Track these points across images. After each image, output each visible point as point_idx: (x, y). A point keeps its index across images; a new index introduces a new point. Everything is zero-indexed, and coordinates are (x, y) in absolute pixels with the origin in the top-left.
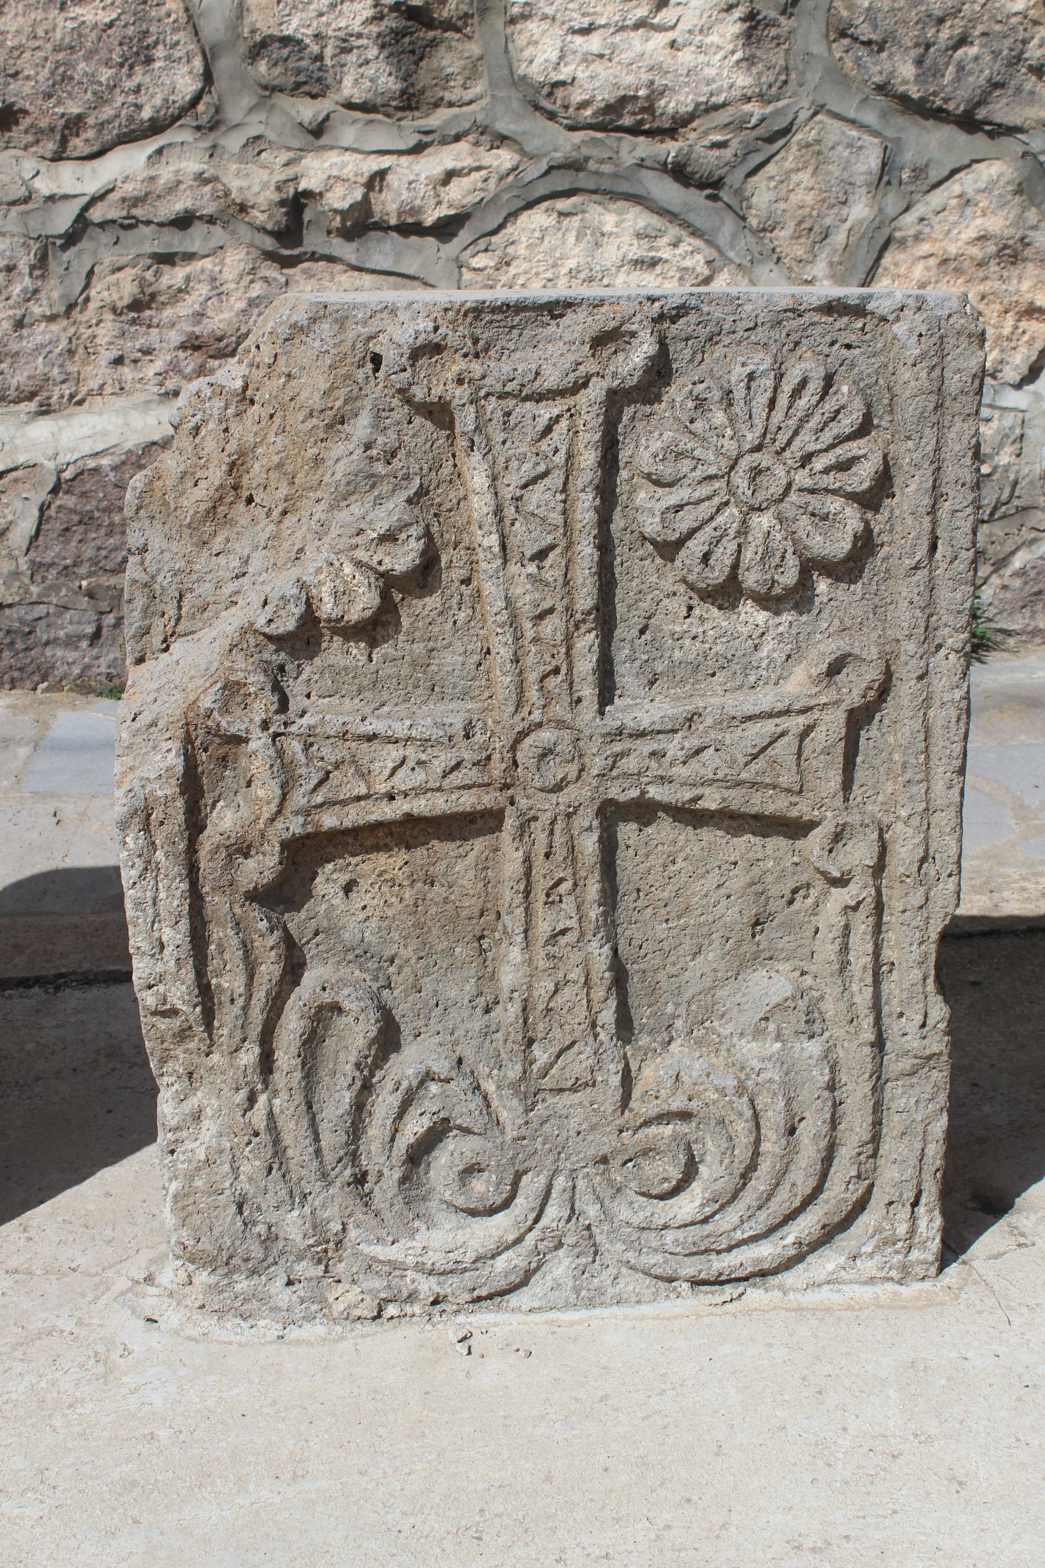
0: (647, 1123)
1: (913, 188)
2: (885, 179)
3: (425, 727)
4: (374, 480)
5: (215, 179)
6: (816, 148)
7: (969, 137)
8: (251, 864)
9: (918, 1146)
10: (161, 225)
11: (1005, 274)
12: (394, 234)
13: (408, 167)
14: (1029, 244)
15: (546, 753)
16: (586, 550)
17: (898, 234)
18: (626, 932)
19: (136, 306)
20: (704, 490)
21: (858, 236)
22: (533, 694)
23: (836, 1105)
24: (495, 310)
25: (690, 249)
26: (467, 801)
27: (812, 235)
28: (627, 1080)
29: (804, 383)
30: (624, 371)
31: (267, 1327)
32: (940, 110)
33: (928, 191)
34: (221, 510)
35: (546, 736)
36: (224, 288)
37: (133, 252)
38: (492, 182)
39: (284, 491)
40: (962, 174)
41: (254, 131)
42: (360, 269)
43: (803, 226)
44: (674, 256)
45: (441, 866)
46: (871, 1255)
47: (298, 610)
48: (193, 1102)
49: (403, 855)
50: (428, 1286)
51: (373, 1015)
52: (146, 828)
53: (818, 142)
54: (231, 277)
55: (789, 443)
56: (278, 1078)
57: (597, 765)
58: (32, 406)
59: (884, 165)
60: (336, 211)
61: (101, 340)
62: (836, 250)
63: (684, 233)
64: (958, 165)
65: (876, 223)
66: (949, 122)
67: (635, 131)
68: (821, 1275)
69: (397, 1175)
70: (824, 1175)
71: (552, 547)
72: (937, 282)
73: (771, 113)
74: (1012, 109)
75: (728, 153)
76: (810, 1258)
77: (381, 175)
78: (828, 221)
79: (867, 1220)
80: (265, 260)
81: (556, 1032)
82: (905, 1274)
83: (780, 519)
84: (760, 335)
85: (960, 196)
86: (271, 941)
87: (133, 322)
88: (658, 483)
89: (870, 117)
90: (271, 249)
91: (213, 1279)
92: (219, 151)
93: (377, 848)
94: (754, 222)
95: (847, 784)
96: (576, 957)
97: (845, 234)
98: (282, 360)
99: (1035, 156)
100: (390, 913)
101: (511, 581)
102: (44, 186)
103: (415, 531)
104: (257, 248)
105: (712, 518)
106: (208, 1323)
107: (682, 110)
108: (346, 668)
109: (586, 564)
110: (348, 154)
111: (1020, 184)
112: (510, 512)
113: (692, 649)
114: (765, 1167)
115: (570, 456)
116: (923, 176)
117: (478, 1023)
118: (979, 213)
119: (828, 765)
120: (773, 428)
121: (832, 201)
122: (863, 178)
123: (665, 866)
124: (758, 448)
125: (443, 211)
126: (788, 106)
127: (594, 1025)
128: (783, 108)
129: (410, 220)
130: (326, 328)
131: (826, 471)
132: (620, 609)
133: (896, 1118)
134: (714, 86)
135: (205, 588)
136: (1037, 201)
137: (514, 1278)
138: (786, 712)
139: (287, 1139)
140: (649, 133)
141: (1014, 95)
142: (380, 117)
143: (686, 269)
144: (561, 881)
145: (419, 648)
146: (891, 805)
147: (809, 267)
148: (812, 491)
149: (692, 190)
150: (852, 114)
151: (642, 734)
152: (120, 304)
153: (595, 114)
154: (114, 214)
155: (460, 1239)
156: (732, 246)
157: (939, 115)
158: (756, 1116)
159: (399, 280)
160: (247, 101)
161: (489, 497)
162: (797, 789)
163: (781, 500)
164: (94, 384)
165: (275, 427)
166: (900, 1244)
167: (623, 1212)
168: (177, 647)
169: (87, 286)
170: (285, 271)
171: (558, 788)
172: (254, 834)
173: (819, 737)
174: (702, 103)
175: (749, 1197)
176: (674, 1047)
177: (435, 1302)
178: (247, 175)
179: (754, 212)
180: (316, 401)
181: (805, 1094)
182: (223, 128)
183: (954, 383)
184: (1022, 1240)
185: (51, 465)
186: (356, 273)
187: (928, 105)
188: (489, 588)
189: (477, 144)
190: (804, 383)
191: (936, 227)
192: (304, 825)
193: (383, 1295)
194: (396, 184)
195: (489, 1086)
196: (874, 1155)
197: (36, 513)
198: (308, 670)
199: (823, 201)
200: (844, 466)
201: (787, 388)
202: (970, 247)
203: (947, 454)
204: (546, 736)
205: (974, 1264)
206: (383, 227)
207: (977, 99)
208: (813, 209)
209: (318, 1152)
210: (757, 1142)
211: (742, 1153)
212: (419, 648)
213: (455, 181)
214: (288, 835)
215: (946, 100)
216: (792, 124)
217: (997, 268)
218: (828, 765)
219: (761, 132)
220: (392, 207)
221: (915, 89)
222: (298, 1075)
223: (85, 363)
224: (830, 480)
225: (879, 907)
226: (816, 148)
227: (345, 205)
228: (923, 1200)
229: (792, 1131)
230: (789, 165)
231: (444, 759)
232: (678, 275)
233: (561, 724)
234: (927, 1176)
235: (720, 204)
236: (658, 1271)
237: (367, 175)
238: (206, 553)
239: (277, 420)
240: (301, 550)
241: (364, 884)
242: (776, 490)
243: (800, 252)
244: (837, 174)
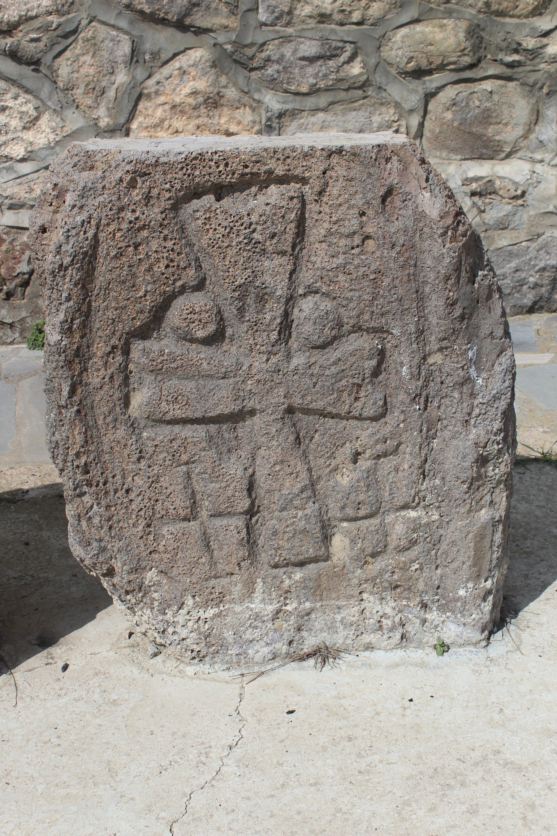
1: (153, 64)
2: (135, 59)
6: (93, 41)
7: (183, 35)
11: (211, 114)
14: (223, 97)
17: (145, 91)
21: (122, 92)
25: (24, 100)
27: (95, 92)
32: (164, 19)
33: (162, 66)
40: (180, 56)
43: (89, 87)
44: (15, 105)
53: (94, 38)
59: (133, 51)
64: (177, 51)
65: (132, 85)
66: (171, 26)
72: (171, 119)
73: (64, 21)
74: (205, 18)
75: (41, 45)
78: (104, 84)
85: (179, 69)
89: (123, 24)
94: (61, 85)
97: (115, 91)
99: (221, 46)
107: (12, 19)
111: (214, 62)
116: (158, 57)
118: (191, 79)
121: (105, 72)
122: (121, 58)
126: (74, 17)
128: (71, 18)
134: (29, 6)
136: (226, 71)
141: (206, 10)
147: (96, 110)
149: (24, 66)
150: (112, 22)
156: (50, 99)
157: (164, 22)
174: (23, 16)
184: (50, 661)
187: (156, 16)
191: (167, 87)
199: (100, 72)
202: (187, 98)
205: (15, 675)
207: (183, 13)
215: (166, 13)
216: (77, 27)
217: (205, 110)
221: (147, 7)
226: (93, 41)
230: (77, 51)
232: (19, 116)
243: (89, 102)
244: (107, 56)
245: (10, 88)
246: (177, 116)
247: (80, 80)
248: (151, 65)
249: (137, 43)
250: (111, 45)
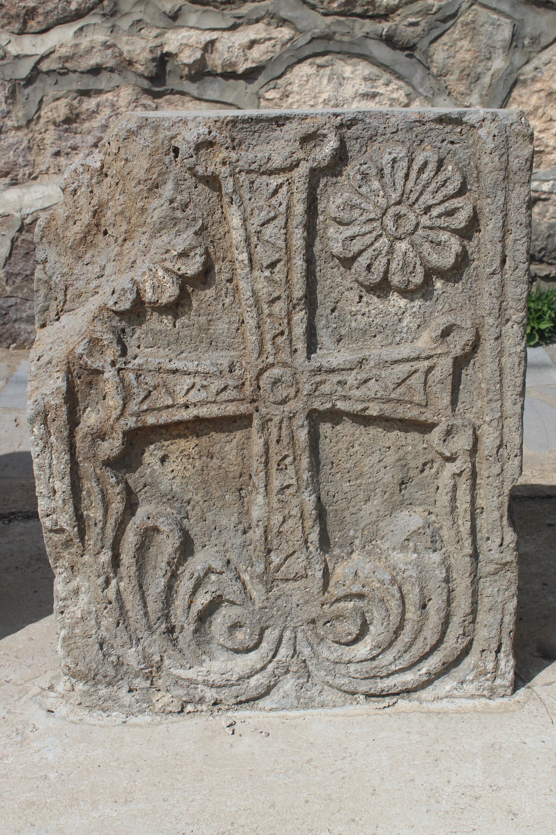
0: (338, 600)
1: (531, 49)
2: (514, 44)
3: (206, 366)
4: (175, 221)
5: (114, 46)
6: (472, 26)
8: (106, 444)
9: (499, 617)
10: (82, 73)
12: (220, 79)
13: (228, 38)
15: (276, 382)
16: (299, 262)
17: (522, 78)
18: (326, 487)
19: (68, 121)
20: (368, 228)
21: (497, 79)
22: (269, 347)
23: (450, 592)
24: (244, 121)
25: (396, 87)
26: (231, 409)
27: (470, 78)
28: (326, 574)
29: (425, 164)
30: (319, 157)
31: (117, 716)
33: (540, 51)
34: (89, 238)
35: (276, 371)
36: (118, 111)
37: (66, 89)
38: (278, 48)
39: (124, 227)
41: (137, 17)
42: (200, 99)
43: (464, 73)
44: (387, 91)
45: (217, 448)
46: (472, 681)
47: (132, 297)
48: (74, 584)
49: (194, 441)
50: (210, 694)
51: (177, 534)
52: (45, 423)
53: (473, 22)
54: (123, 104)
55: (417, 200)
56: (123, 570)
57: (306, 388)
58: (7, 180)
59: (513, 35)
60: (185, 65)
61: (48, 142)
62: (484, 88)
63: (392, 78)
65: (508, 71)
67: (363, 16)
68: (442, 693)
69: (192, 628)
70: (443, 633)
71: (279, 261)
72: (545, 106)
73: (445, 5)
75: (419, 29)
76: (436, 683)
77: (212, 43)
78: (479, 70)
79: (470, 660)
80: (144, 94)
81: (284, 546)
82: (492, 693)
83: (412, 244)
84: (400, 136)
86: (118, 489)
87: (66, 131)
88: (340, 223)
90: (147, 87)
91: (86, 688)
92: (116, 29)
93: (179, 436)
94: (434, 71)
95: (454, 402)
96: (295, 501)
98: (122, 151)
100: (187, 474)
101: (255, 280)
102: (13, 50)
103: (199, 251)
104: (139, 87)
105: (372, 244)
106: (83, 713)
108: (160, 331)
109: (299, 270)
110: (192, 30)
112: (254, 240)
113: (363, 321)
114: (408, 627)
115: (288, 207)
116: (537, 42)
117: (239, 540)
119: (443, 390)
120: (408, 191)
121: (482, 58)
122: (500, 43)
123: (348, 449)
124: (399, 203)
125: (249, 65)
127: (306, 542)
129: (229, 70)
130: (147, 132)
131: (439, 216)
132: (320, 297)
133: (486, 600)
135: (80, 284)
137: (261, 690)
138: (418, 358)
139: (128, 606)
140: (372, 17)
142: (211, 8)
143: (394, 99)
144: (286, 457)
145: (203, 319)
146: (480, 414)
147: (468, 98)
148: (431, 228)
149: (398, 52)
151: (333, 371)
152: (58, 120)
153: (339, 6)
154: (54, 66)
155: (229, 666)
158: (402, 597)
159: (223, 106)
161: (242, 231)
162: (424, 404)
163: (413, 234)
164: (43, 167)
165: (119, 190)
166: (489, 675)
167: (325, 653)
168: (64, 318)
169: (39, 109)
170: (156, 100)
171: (284, 402)
172: (107, 427)
173: (437, 374)
175: (399, 645)
176: (354, 556)
177: (215, 704)
178: (133, 43)
179: (434, 64)
180: (142, 175)
181: (432, 585)
182: (119, 15)
183: (515, 164)
185: (18, 215)
186: (198, 102)
188: (242, 284)
189: (269, 24)
190: (425, 164)
191: (545, 73)
192: (136, 422)
193: (184, 699)
194: (221, 48)
195: (246, 577)
196: (473, 622)
197: (9, 243)
198: (138, 331)
199: (477, 57)
200: (450, 213)
201: (416, 167)
203: (511, 206)
204: (276, 371)
205: (535, 688)
206: (213, 74)
208: (470, 62)
209: (146, 614)
210: (403, 613)
211: (394, 619)
212: (203, 319)
213: (256, 47)
214: (126, 428)
216: (457, 11)
218: (443, 390)
219: (439, 16)
220: (219, 62)
222: (134, 568)
223: (38, 154)
224: (441, 222)
225: (474, 475)
226: (472, 26)
227: (191, 61)
228: (503, 649)
229: (424, 606)
230: (455, 36)
231: (216, 385)
232: (389, 103)
233: (285, 365)
234: (505, 635)
235: (414, 60)
236: (345, 688)
237: (203, 43)
238: (80, 263)
239: (120, 186)
240: (134, 262)
241: (172, 457)
242: (410, 227)
243: (462, 88)
244: (485, 41)
245: (382, 74)
246: (551, 104)
247: (456, 66)
248: (530, 49)
249: (518, 26)
250: (490, 29)
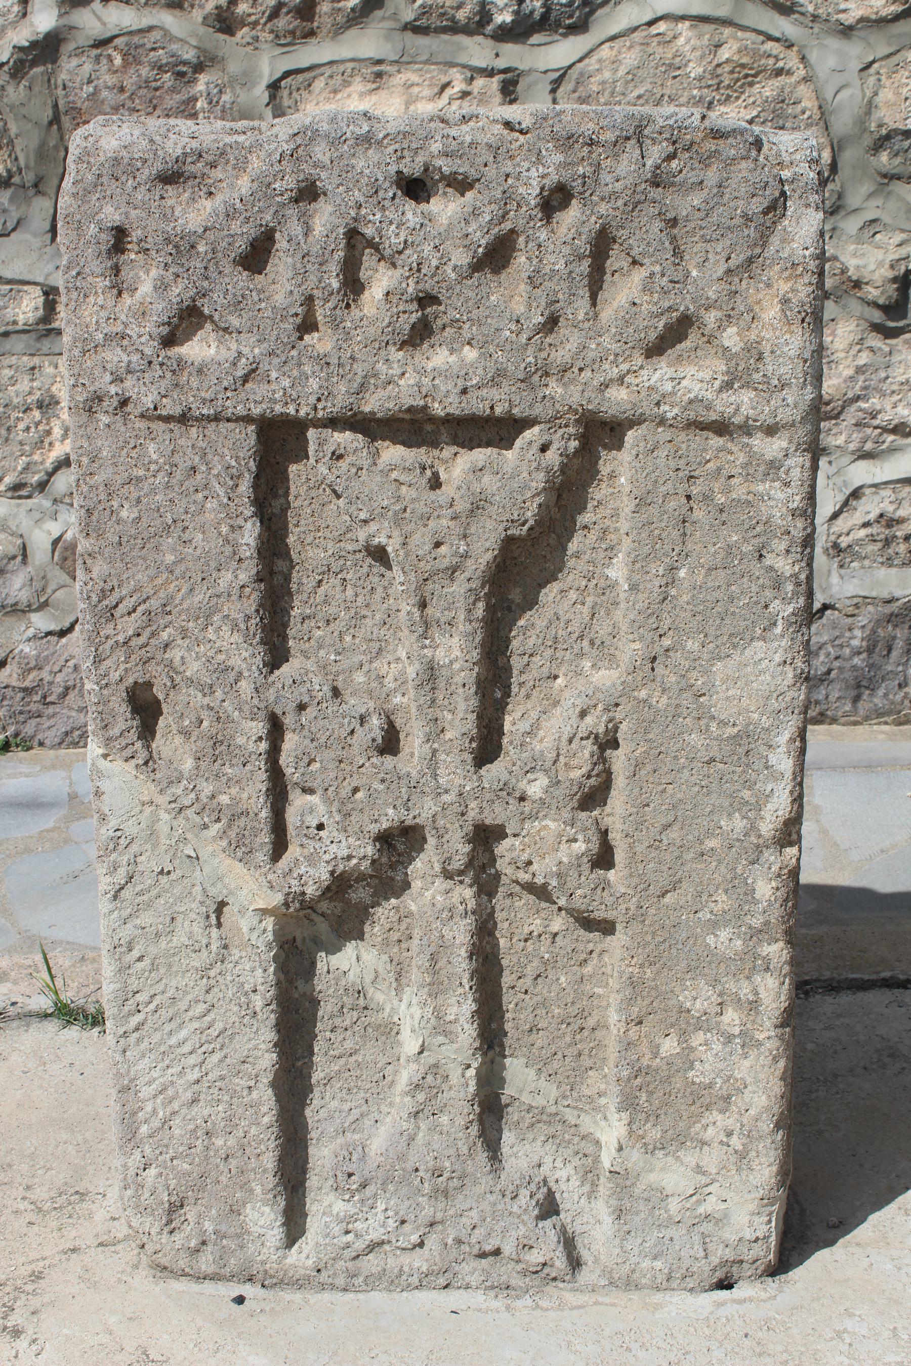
36: (833, 357)
54: (841, 347)
80: (872, 331)
90: (878, 321)
92: (838, 232)
104: (866, 320)
160: (867, 187)
170: (888, 341)
178: (864, 254)
182: (843, 213)
